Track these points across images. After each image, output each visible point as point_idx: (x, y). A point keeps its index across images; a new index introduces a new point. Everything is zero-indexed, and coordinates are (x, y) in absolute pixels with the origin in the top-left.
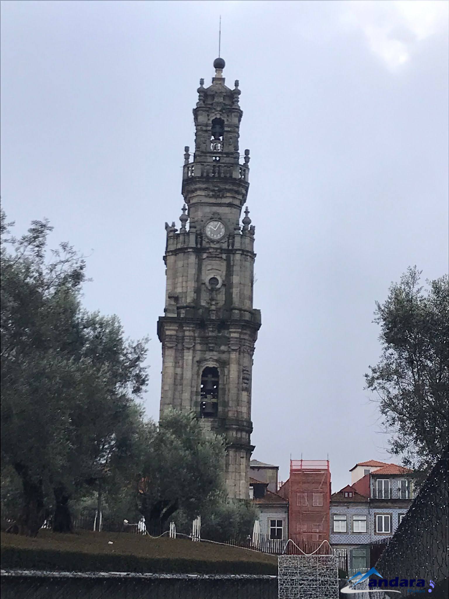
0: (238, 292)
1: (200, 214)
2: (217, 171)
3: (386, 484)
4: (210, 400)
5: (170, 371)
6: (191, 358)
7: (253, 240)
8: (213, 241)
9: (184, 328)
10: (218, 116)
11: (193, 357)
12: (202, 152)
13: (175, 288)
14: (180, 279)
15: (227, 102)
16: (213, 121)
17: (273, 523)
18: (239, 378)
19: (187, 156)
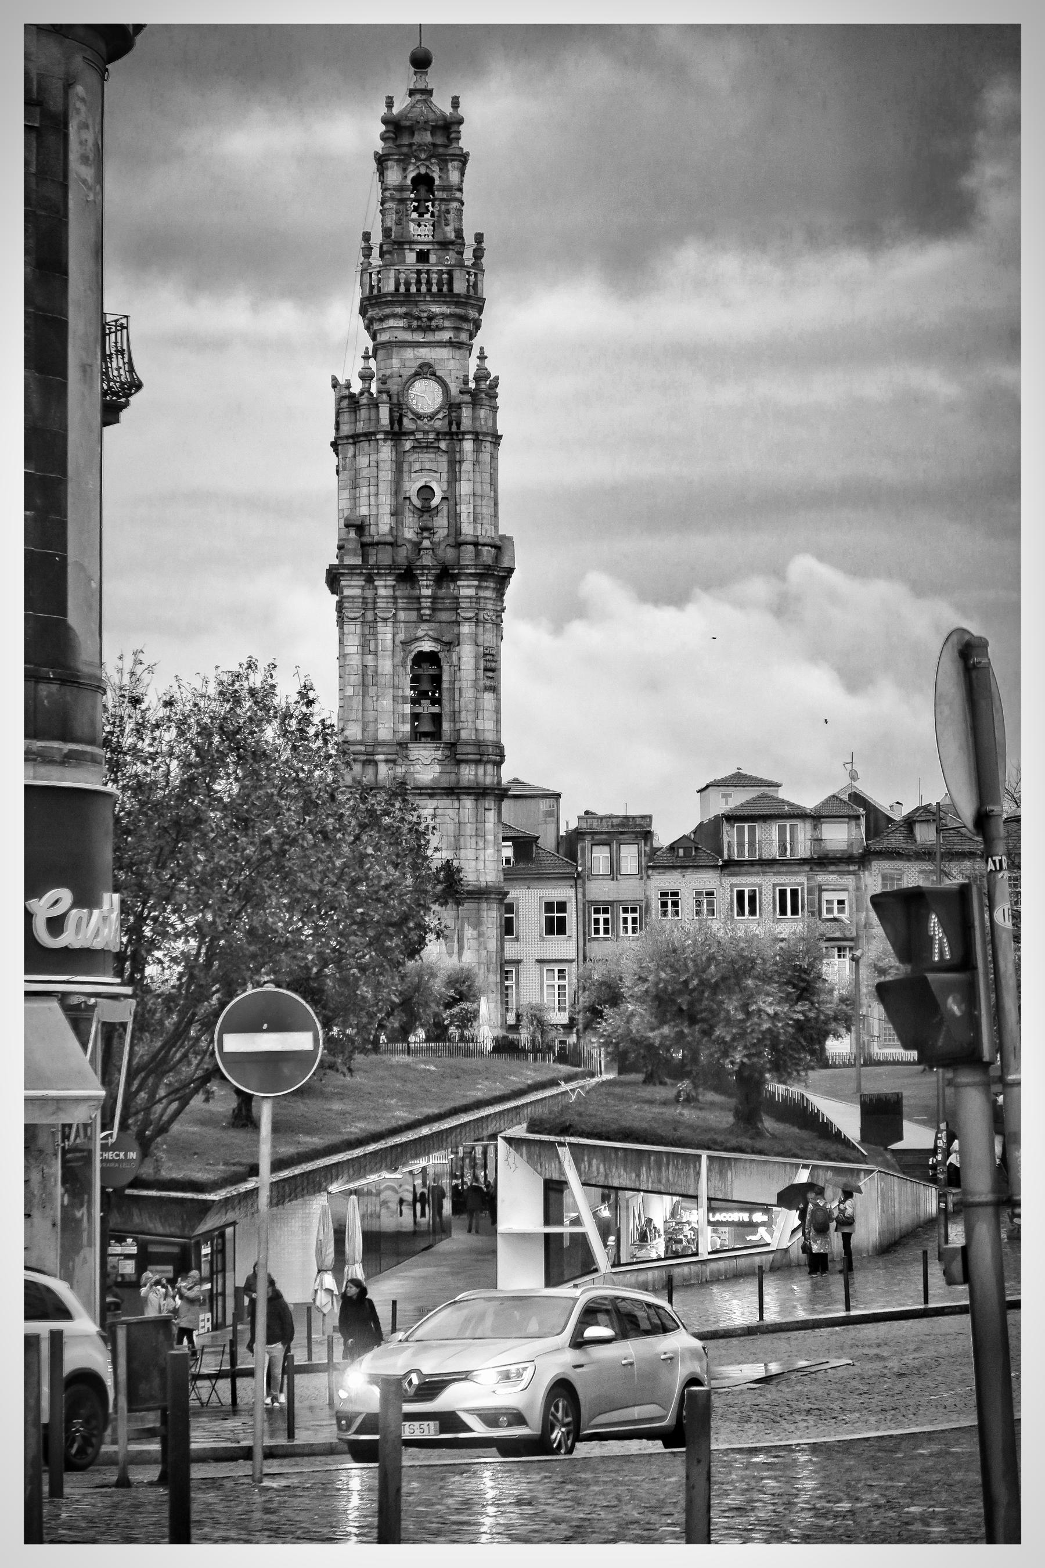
0: (472, 510)
1: (395, 362)
2: (424, 281)
3: (752, 830)
4: (426, 708)
5: (355, 661)
6: (390, 636)
7: (495, 409)
8: (419, 417)
9: (376, 583)
10: (423, 170)
11: (394, 635)
12: (395, 243)
13: (355, 506)
14: (365, 491)
15: (439, 140)
16: (413, 180)
17: (549, 907)
18: (477, 669)
19: (367, 252)
